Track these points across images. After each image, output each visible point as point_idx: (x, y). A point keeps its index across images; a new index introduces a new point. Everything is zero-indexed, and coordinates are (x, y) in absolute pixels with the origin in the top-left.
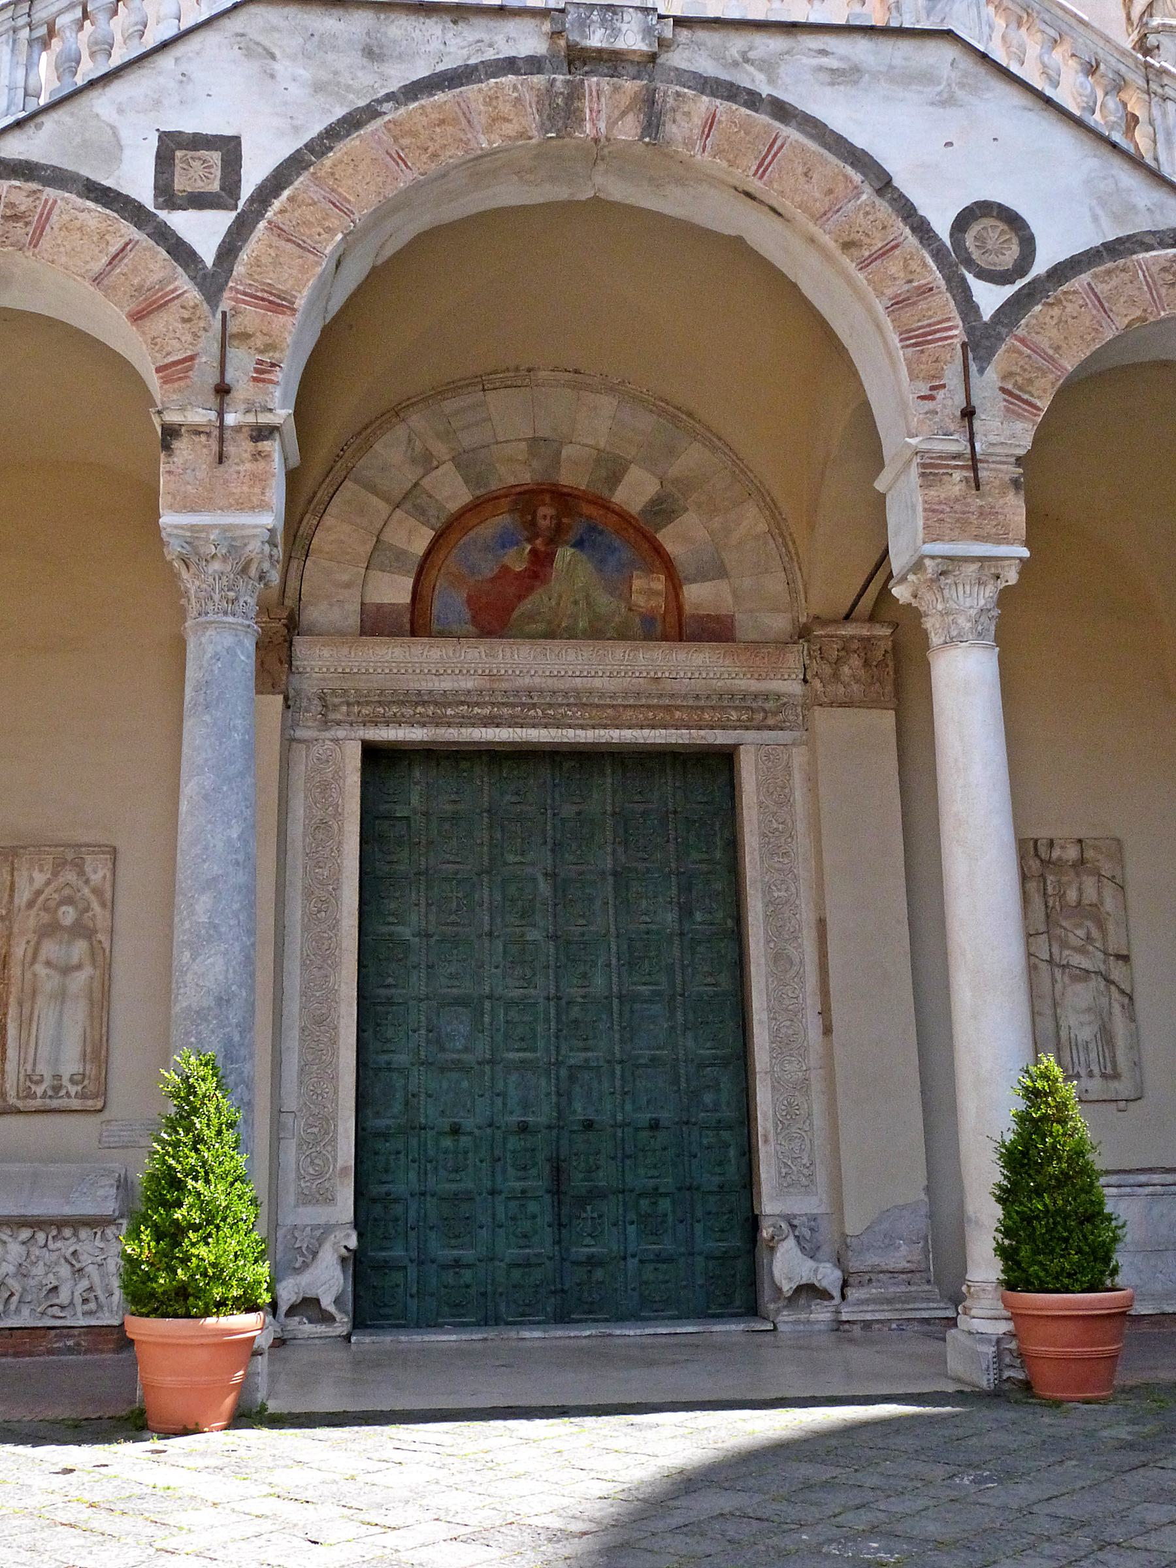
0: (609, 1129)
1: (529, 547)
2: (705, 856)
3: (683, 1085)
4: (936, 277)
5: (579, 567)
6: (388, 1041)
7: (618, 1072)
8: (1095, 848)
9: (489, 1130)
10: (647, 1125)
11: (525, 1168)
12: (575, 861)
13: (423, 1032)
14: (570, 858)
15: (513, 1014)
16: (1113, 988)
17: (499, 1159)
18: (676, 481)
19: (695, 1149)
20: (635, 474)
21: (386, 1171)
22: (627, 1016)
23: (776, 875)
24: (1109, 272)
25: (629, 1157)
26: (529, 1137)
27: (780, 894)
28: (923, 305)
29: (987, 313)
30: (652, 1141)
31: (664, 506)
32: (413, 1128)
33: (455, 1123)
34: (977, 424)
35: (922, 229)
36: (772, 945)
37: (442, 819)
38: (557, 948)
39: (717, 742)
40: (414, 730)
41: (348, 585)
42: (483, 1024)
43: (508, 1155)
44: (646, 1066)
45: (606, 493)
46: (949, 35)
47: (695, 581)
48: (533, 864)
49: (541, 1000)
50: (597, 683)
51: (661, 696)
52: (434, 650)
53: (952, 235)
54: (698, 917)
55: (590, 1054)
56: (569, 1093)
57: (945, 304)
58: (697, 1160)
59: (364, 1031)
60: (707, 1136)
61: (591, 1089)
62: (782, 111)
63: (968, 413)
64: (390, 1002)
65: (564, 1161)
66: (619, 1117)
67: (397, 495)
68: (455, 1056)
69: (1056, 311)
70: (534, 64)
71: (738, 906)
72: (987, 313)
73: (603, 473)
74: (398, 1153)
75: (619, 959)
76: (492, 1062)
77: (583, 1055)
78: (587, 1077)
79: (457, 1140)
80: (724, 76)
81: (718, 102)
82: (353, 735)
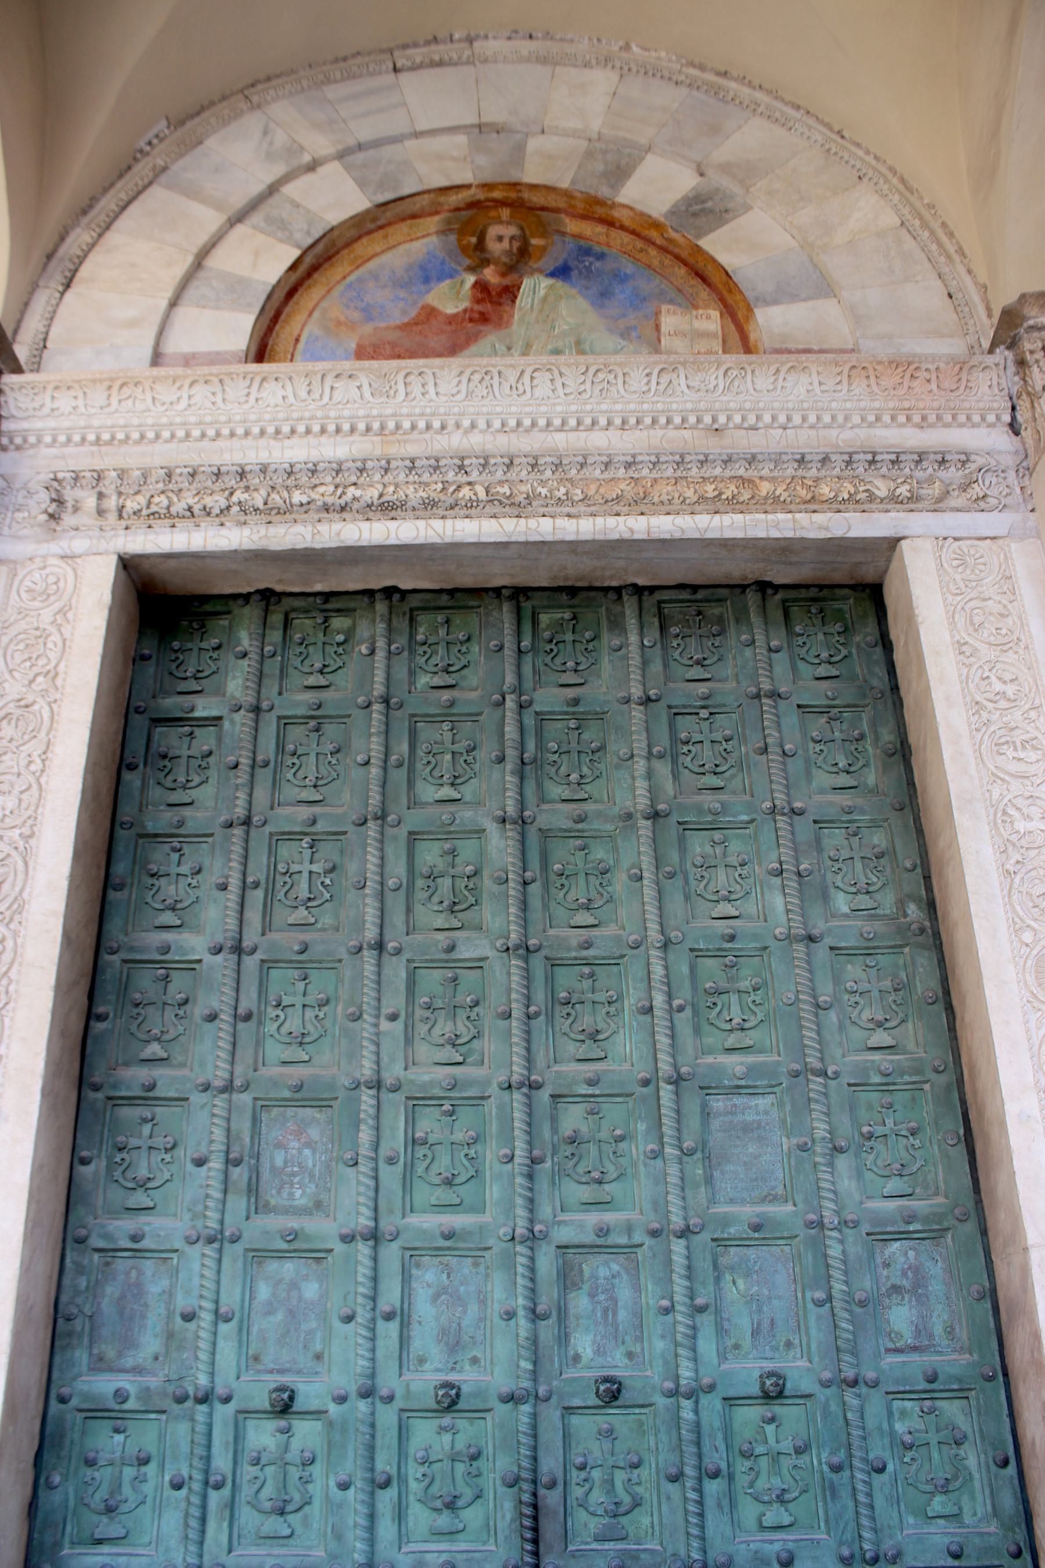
0: (661, 1401)
1: (471, 279)
2: (844, 780)
3: (838, 1287)
5: (563, 304)
6: (143, 1185)
7: (679, 1259)
9: (363, 1406)
10: (756, 1390)
11: (451, 1505)
12: (567, 794)
13: (216, 1164)
14: (556, 791)
15: (429, 1123)
17: (386, 1484)
18: (726, 168)
19: (879, 1450)
20: (652, 166)
21: (110, 1510)
22: (694, 1122)
23: (1016, 786)
25: (715, 1475)
26: (461, 1424)
27: (1031, 826)
30: (770, 1429)
31: (709, 204)
32: (181, 1400)
33: (281, 1389)
36: (1027, 937)
37: (285, 722)
38: (528, 977)
39: (853, 534)
40: (224, 531)
41: (132, 324)
42: (356, 1144)
43: (414, 1471)
44: (742, 1242)
45: (604, 191)
47: (775, 302)
48: (478, 804)
49: (493, 1090)
50: (598, 440)
51: (727, 461)
52: (270, 386)
54: (842, 903)
55: (609, 1217)
56: (562, 1313)
58: (884, 1477)
59: (84, 1162)
60: (903, 1413)
61: (615, 1301)
64: (148, 1095)
65: (552, 1485)
66: (686, 1373)
67: (238, 200)
68: (293, 1223)
71: (927, 878)
73: (599, 167)
74: (145, 1461)
75: (670, 996)
76: (374, 1236)
77: (593, 1218)
78: (603, 1272)
79: (287, 1431)
82: (103, 546)
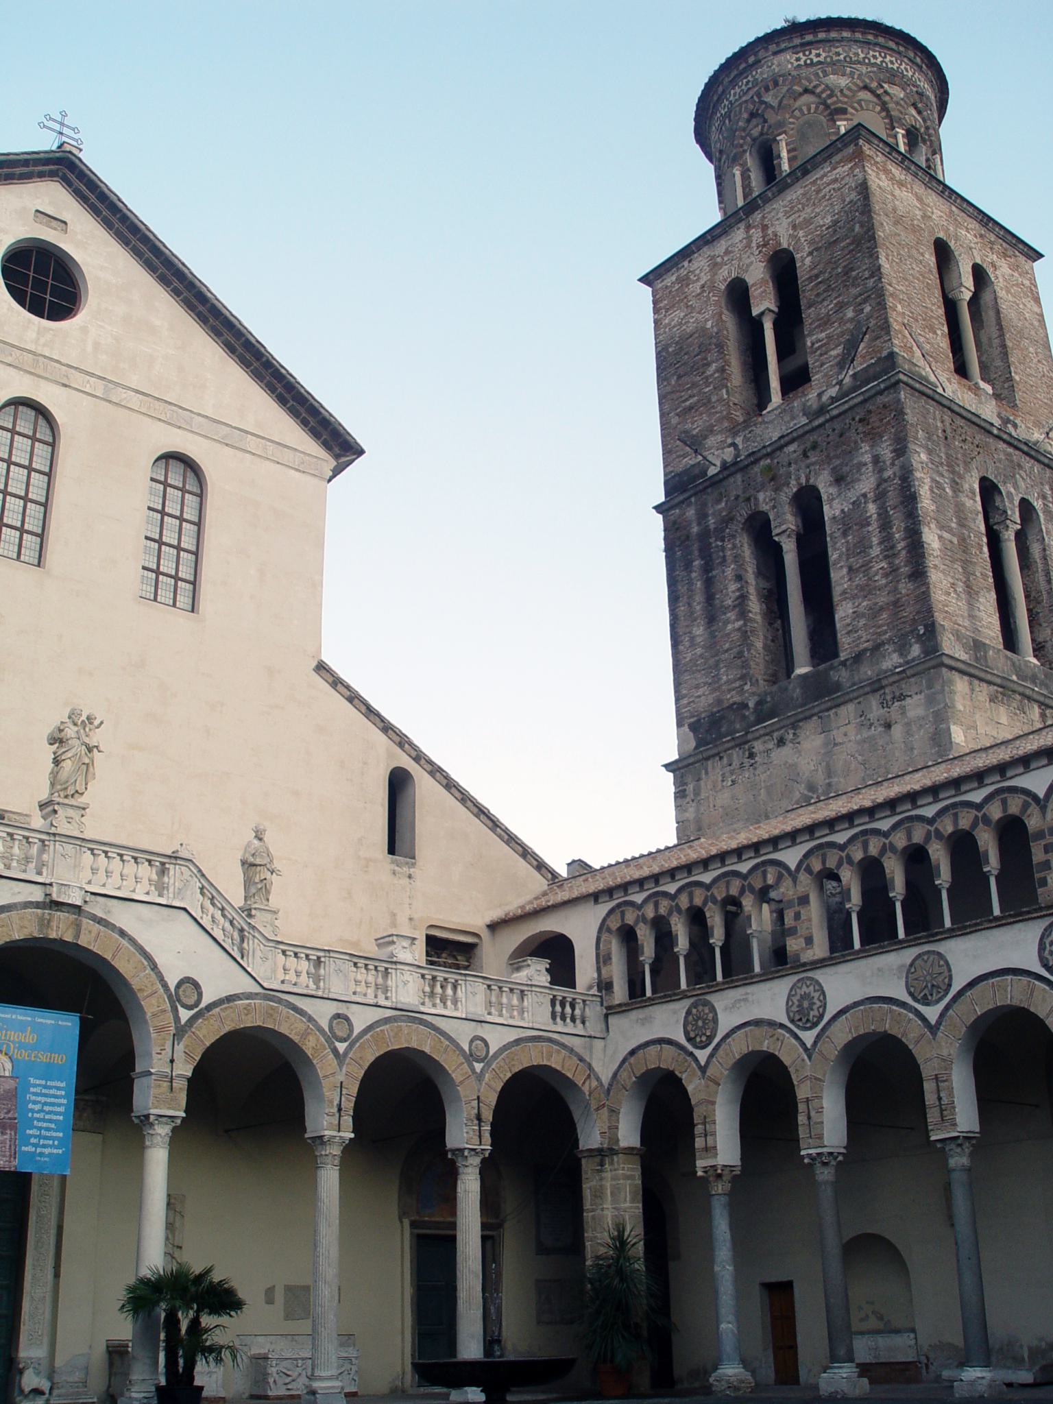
4: (168, 1006)
8: (175, 1198)
16: (174, 1261)
24: (226, 1008)
28: (162, 1017)
29: (183, 1022)
34: (174, 1064)
35: (165, 986)
46: (185, 909)
53: (175, 990)
57: (170, 1015)
62: (122, 933)
63: (172, 1061)
69: (206, 1022)
70: (37, 905)
72: (183, 1022)
80: (104, 917)
81: (101, 927)
